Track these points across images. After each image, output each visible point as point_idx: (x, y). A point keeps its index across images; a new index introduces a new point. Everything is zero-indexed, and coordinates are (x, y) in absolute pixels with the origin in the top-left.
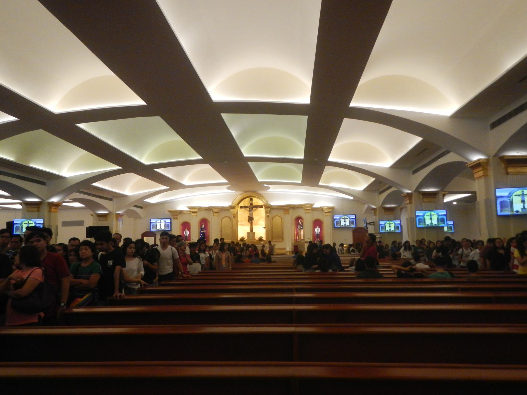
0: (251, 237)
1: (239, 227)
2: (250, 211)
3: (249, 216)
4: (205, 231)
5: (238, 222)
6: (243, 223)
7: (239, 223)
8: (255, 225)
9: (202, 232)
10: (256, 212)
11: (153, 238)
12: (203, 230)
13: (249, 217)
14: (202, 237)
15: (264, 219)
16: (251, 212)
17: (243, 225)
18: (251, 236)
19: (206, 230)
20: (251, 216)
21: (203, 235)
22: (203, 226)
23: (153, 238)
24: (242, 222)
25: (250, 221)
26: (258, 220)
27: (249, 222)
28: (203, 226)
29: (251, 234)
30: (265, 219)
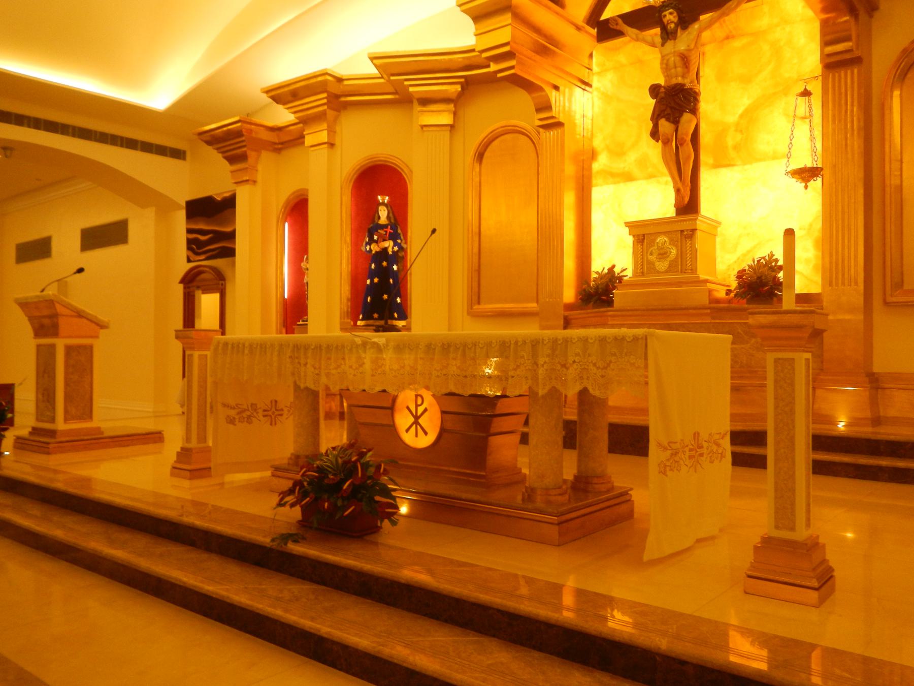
0: (662, 265)
1: (600, 194)
2: (668, 35)
3: (661, 81)
4: (389, 244)
5: (593, 155)
6: (629, 161)
7: (596, 166)
8: (717, 165)
9: (375, 248)
10: (737, 43)
11: (216, 296)
12: (376, 242)
13: (654, 90)
14: (372, 281)
15: (806, 93)
16: (683, 42)
17: (628, 177)
18: (663, 255)
19: (394, 237)
20: (680, 80)
21: (384, 274)
22: (383, 213)
23: (216, 296)
24: (618, 152)
25: (665, 126)
26: (750, 117)
27: (655, 134)
28: (383, 213)
29: (661, 239)
30: (816, 88)
